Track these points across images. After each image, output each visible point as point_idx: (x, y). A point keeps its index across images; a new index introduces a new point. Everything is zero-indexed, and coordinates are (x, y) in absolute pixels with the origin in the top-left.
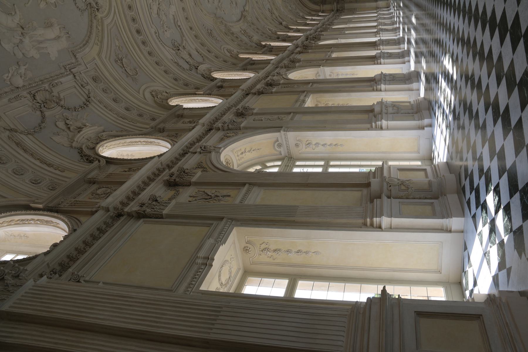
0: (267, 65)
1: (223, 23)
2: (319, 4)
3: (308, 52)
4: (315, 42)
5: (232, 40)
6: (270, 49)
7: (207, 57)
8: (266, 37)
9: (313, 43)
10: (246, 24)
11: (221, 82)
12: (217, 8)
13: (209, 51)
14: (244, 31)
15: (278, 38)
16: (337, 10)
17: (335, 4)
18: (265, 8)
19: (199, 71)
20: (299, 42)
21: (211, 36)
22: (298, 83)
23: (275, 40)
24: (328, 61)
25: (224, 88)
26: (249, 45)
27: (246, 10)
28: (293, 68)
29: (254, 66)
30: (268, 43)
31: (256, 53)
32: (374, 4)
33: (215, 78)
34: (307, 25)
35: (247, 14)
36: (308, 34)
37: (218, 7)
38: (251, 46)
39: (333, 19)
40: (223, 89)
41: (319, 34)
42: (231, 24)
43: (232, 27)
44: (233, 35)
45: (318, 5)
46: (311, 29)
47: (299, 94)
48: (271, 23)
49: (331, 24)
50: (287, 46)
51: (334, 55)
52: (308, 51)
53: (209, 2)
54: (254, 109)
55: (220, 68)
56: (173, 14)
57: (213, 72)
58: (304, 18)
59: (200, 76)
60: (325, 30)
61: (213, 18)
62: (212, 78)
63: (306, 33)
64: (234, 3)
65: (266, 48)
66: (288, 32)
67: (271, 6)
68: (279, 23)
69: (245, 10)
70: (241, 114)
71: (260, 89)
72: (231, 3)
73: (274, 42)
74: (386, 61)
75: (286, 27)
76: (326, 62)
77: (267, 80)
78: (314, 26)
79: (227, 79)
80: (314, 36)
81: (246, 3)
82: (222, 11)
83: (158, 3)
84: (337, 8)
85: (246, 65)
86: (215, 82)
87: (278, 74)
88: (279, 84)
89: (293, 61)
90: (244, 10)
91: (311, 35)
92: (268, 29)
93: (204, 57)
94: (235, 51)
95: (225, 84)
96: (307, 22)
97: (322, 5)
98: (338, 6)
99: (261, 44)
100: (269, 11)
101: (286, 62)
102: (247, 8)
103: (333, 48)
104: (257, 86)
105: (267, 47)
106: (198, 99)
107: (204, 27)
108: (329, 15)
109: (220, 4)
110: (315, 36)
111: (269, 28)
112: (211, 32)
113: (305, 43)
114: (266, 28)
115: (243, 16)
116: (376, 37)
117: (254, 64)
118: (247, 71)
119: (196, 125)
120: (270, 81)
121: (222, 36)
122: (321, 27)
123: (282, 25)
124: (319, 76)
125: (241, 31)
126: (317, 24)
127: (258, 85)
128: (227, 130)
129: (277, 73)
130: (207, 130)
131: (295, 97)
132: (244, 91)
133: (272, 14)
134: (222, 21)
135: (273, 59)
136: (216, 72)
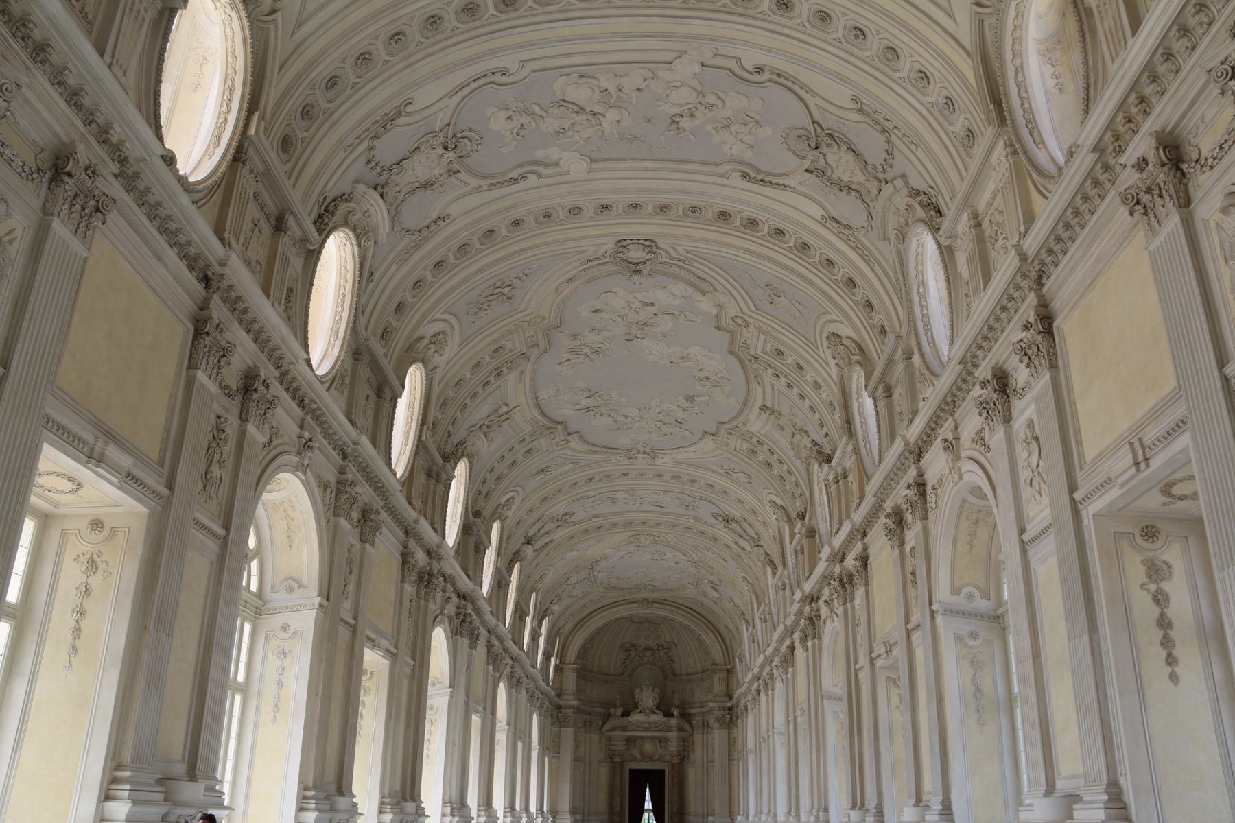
1: (532, 347)
10: (530, 429)
14: (505, 417)
27: (570, 438)
34: (518, 615)
42: (528, 375)
43: (520, 379)
56: (561, 163)
61: (547, 316)
64: (588, 402)
72: (590, 391)
75: (517, 552)
83: (598, 109)
92: (513, 498)
98: (571, 711)
107: (521, 275)
111: (515, 502)
123: (523, 544)
125: (507, 405)
134: (538, 345)
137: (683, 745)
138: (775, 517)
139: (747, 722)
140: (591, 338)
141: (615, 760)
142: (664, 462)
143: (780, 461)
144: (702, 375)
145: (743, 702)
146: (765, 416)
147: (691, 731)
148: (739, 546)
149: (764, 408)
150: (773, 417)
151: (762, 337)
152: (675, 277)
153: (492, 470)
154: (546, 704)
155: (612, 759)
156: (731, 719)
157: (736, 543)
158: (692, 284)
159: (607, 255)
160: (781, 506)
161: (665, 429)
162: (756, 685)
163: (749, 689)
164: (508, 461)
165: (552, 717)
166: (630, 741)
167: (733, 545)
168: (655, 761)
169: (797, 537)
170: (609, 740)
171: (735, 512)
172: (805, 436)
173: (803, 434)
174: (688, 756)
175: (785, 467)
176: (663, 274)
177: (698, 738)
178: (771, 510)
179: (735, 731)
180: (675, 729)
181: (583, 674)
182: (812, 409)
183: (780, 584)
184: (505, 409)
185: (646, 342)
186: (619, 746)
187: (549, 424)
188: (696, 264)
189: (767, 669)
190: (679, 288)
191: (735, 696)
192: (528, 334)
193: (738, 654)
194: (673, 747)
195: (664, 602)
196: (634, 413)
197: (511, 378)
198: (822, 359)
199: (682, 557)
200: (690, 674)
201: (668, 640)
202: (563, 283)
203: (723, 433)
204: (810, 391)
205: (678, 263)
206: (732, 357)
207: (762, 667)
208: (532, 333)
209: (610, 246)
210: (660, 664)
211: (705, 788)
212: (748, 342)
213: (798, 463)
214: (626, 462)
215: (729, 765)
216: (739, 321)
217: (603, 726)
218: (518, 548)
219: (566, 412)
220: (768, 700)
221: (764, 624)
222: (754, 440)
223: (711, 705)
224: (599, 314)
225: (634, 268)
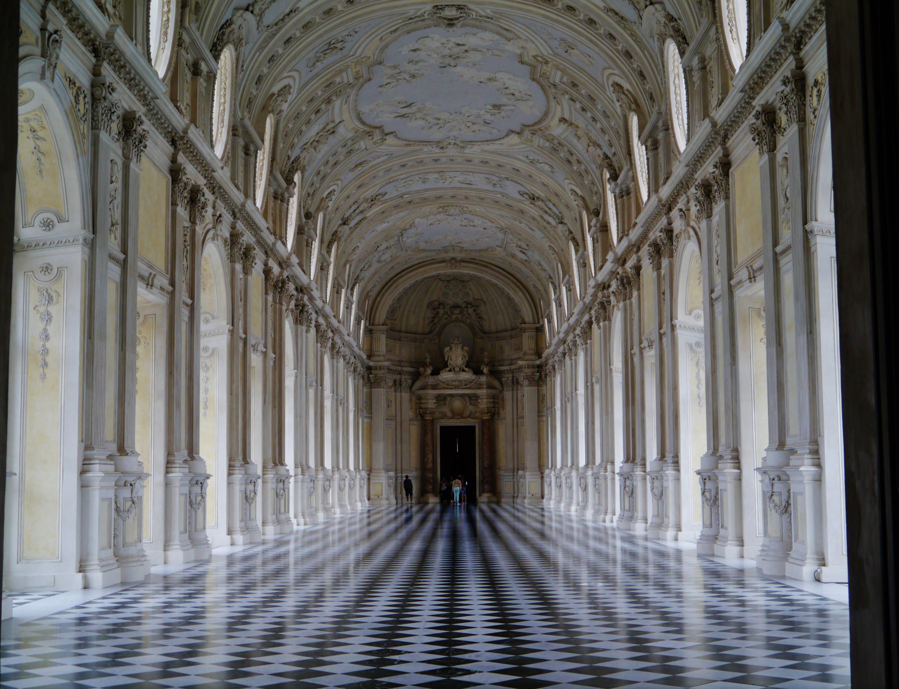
0: (241, 187)
2: (388, 322)
3: (266, 293)
4: (292, 311)
5: (312, 100)
6: (282, 195)
7: (274, 35)
8: (313, 184)
9: (288, 305)
11: (207, 72)
12: (395, 67)
13: (288, 41)
14: (332, 130)
15: (308, 216)
16: (369, 369)
17: (387, 363)
18: (387, 184)
19: (242, 15)
20: (298, 271)
21: (326, 47)
22: (193, 269)
23: (304, 207)
24: (241, 345)
25: (192, 79)
26: (296, 140)
27: (387, 137)
28: (231, 256)
29: (241, 153)
30: (296, 190)
31: (273, 159)
32: (380, 461)
33: (219, 55)
34: (336, 289)
35: (375, 139)
36: (312, 293)
37: (398, 71)
38: (292, 146)
39: (348, 358)
40: (189, 75)
41: (311, 320)
44: (325, 102)
45: (387, 318)
46: (324, 299)
47: (167, 273)
48: (348, 197)
49: (335, 351)
50: (286, 238)
51: (256, 360)
52: (269, 292)
53: (412, 50)
54: (139, 160)
55: (242, 66)
57: (236, 49)
58: (357, 280)
59: (228, 16)
60: (321, 335)
62: (219, 48)
63: (317, 288)
65: (284, 185)
66: (322, 242)
67: (392, 199)
68: (346, 216)
69: (386, 135)
70: (129, 124)
71: (185, 174)
73: (299, 206)
74: (238, 489)
75: (335, 234)
76: (241, 338)
77: (206, 190)
78: (332, 308)
79: (214, 87)
80: (306, 309)
81: (402, 140)
82: (389, 81)
84: (376, 368)
85: (246, 133)
86: (209, 56)
87: (218, 219)
88: (193, 222)
89: (247, 255)
90: (386, 131)
91: (311, 299)
93: (275, 28)
94: (285, 107)
95: (201, 80)
96: (343, 291)
97: (387, 330)
99: (297, 170)
100: (380, 194)
101: (244, 238)
102: (390, 140)
103: (274, 356)
104: (191, 166)
105: (287, 188)
106: (169, 11)
108: (358, 345)
109: (407, 77)
110: (307, 312)
111: (335, 193)
112: (337, 48)
113: (291, 287)
114: (337, 185)
115: (373, 130)
116: (296, 467)
117: (247, 154)
118: (230, 138)
119: (109, 16)
120: (203, 199)
121: (323, 77)
122: (329, 325)
123: (340, 225)
124: (207, 321)
126: (336, 316)
127: (194, 170)
128: (92, 94)
129: (220, 216)
130: (97, 43)
131: (160, 261)
132: (182, 134)
133: (372, 201)
135: (255, 204)
136: (234, 57)
137: (494, 402)
138: (576, 203)
139: (554, 381)
140: (412, 68)
141: (426, 418)
142: (473, 151)
143: (579, 162)
144: (508, 91)
145: (550, 361)
146: (563, 126)
147: (500, 388)
148: (545, 220)
149: (563, 120)
150: (570, 128)
151: (559, 73)
152: (485, 29)
153: (319, 173)
154: (360, 368)
156: (540, 376)
157: (541, 217)
158: (497, 34)
159: (426, 15)
160: (581, 196)
161: (475, 127)
162: (561, 349)
163: (556, 351)
164: (332, 162)
165: (363, 379)
166: (440, 399)
167: (539, 219)
168: (465, 418)
169: (593, 229)
171: (539, 192)
172: (598, 149)
173: (596, 147)
175: (583, 167)
176: (474, 26)
177: (508, 395)
178: (572, 197)
179: (544, 388)
180: (485, 386)
181: (395, 334)
182: (603, 130)
183: (581, 261)
184: (332, 125)
185: (458, 69)
186: (431, 404)
187: (368, 129)
188: (501, 21)
189: (571, 337)
190: (488, 36)
191: (544, 355)
192: (354, 70)
193: (546, 315)
194: (484, 404)
195: (472, 261)
196: (445, 116)
197: (337, 103)
198: (609, 97)
199: (489, 224)
200: (501, 332)
201: (476, 297)
202: (387, 33)
203: (527, 133)
204: (600, 117)
205: (487, 20)
206: (535, 84)
207: (567, 333)
208: (358, 68)
209: (429, 7)
210: (469, 321)
212: (548, 73)
213: (594, 167)
214: (438, 150)
215: (539, 422)
216: (539, 59)
217: (413, 383)
218: (335, 229)
219: (387, 119)
220: (572, 363)
221: (568, 293)
222: (556, 142)
223: (521, 363)
224: (418, 52)
225: (448, 22)
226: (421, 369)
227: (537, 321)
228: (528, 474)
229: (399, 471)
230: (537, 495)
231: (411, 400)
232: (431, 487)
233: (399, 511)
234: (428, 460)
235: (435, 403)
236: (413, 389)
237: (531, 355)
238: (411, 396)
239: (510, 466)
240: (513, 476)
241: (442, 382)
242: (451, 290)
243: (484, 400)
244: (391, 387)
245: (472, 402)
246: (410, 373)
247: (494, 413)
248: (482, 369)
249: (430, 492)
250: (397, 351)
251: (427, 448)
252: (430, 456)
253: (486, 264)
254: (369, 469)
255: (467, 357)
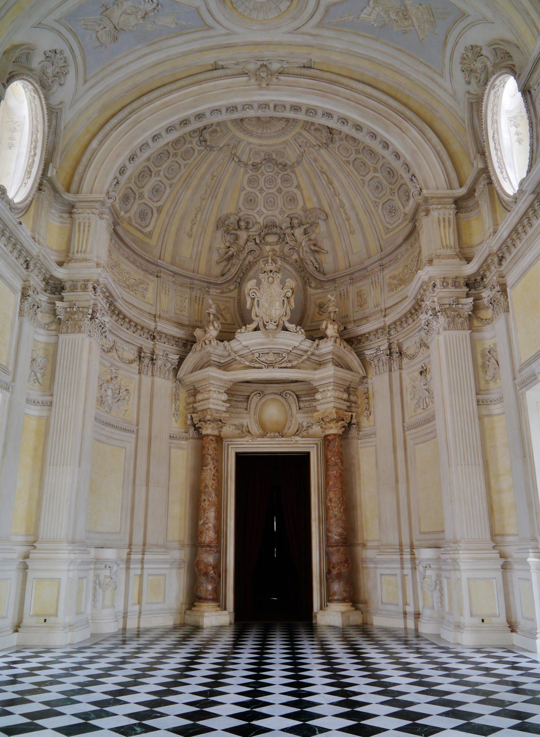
141: (204, 432)
147: (362, 373)
155: (197, 429)
170: (194, 392)
174: (358, 424)
201: (309, 206)
211: (402, 487)
217: (181, 360)
226: (198, 333)
227: (456, 184)
228: (463, 556)
229: (137, 548)
230: (495, 620)
231: (176, 397)
232: (210, 587)
233: (130, 648)
234: (204, 524)
235: (224, 401)
236: (181, 374)
237: (449, 257)
238: (177, 388)
239: (392, 538)
240: (402, 561)
241: (241, 356)
242: (261, 191)
243: (329, 394)
244: (131, 362)
245: (302, 405)
246: (176, 340)
247: (350, 424)
248: (324, 326)
249: (206, 600)
250: (150, 295)
251: (203, 497)
252: (211, 514)
253: (334, 77)
254: (31, 539)
255: (292, 300)
